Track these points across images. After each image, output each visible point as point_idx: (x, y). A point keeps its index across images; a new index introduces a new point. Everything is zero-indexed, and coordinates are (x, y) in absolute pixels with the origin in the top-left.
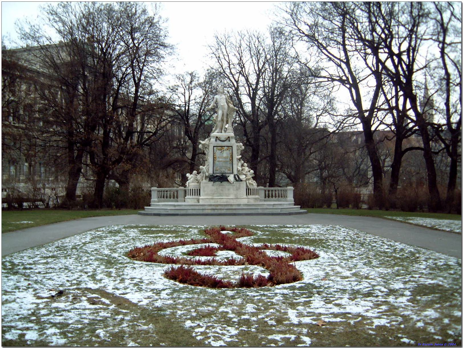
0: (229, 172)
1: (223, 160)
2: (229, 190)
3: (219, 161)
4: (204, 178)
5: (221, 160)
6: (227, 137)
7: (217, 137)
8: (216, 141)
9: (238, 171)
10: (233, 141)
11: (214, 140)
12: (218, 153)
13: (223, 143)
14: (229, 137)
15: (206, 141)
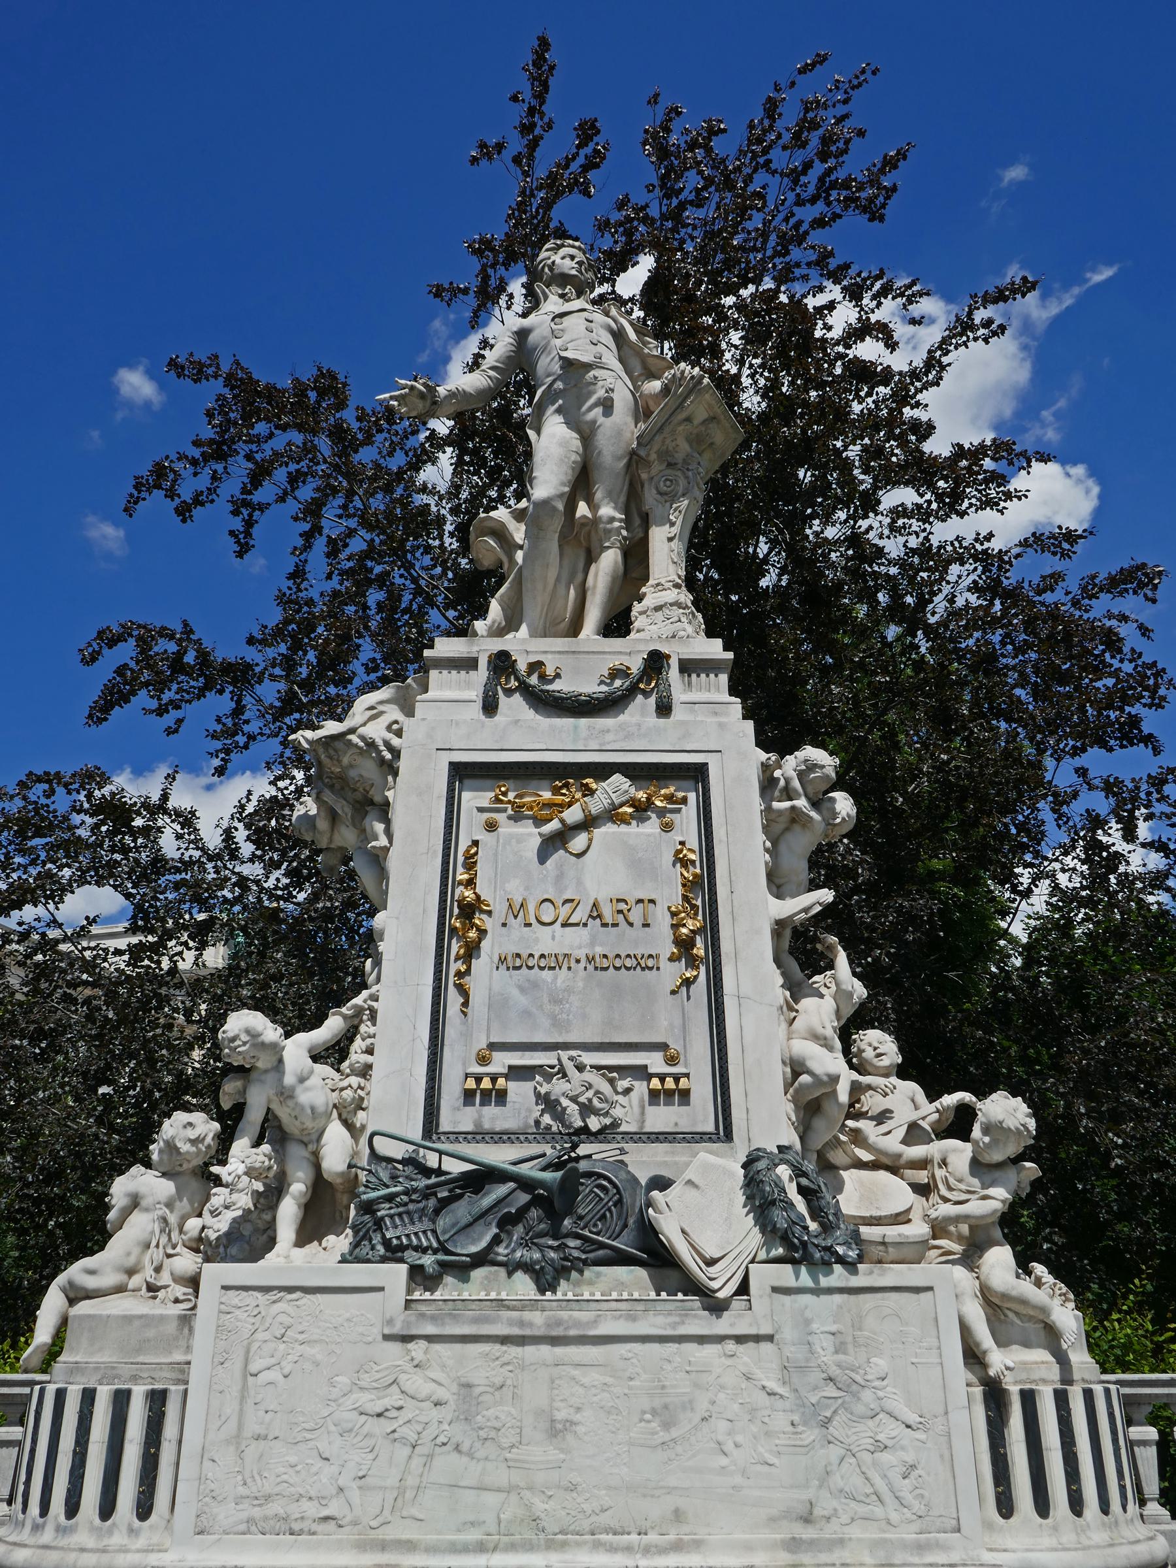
0: (662, 1118)
1: (575, 941)
2: (665, 1415)
3: (512, 963)
4: (288, 1212)
5: (546, 941)
6: (636, 665)
7: (502, 663)
8: (490, 707)
9: (811, 1106)
10: (712, 724)
11: (475, 693)
12: (508, 854)
13: (583, 722)
14: (656, 662)
15: (370, 715)
